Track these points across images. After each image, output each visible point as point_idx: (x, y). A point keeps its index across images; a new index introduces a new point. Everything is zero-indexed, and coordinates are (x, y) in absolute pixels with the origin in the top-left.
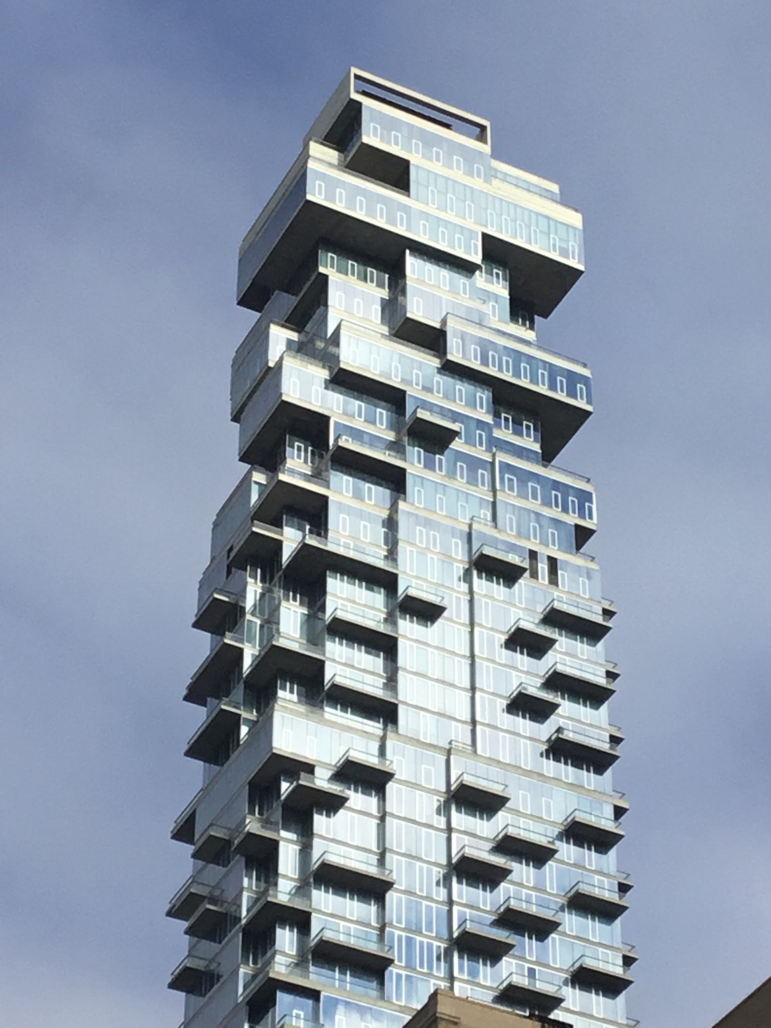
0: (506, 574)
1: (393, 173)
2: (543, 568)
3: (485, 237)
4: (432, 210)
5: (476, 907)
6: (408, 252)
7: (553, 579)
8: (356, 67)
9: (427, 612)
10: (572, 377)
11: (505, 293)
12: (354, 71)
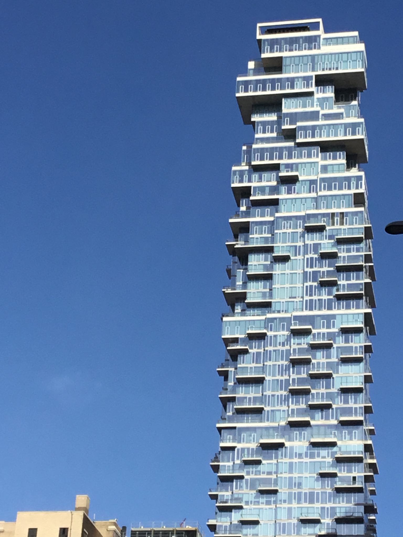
0: (321, 229)
1: (276, 65)
2: (337, 220)
6: (283, 99)
9: (285, 259)
11: (333, 95)
12: (259, 25)
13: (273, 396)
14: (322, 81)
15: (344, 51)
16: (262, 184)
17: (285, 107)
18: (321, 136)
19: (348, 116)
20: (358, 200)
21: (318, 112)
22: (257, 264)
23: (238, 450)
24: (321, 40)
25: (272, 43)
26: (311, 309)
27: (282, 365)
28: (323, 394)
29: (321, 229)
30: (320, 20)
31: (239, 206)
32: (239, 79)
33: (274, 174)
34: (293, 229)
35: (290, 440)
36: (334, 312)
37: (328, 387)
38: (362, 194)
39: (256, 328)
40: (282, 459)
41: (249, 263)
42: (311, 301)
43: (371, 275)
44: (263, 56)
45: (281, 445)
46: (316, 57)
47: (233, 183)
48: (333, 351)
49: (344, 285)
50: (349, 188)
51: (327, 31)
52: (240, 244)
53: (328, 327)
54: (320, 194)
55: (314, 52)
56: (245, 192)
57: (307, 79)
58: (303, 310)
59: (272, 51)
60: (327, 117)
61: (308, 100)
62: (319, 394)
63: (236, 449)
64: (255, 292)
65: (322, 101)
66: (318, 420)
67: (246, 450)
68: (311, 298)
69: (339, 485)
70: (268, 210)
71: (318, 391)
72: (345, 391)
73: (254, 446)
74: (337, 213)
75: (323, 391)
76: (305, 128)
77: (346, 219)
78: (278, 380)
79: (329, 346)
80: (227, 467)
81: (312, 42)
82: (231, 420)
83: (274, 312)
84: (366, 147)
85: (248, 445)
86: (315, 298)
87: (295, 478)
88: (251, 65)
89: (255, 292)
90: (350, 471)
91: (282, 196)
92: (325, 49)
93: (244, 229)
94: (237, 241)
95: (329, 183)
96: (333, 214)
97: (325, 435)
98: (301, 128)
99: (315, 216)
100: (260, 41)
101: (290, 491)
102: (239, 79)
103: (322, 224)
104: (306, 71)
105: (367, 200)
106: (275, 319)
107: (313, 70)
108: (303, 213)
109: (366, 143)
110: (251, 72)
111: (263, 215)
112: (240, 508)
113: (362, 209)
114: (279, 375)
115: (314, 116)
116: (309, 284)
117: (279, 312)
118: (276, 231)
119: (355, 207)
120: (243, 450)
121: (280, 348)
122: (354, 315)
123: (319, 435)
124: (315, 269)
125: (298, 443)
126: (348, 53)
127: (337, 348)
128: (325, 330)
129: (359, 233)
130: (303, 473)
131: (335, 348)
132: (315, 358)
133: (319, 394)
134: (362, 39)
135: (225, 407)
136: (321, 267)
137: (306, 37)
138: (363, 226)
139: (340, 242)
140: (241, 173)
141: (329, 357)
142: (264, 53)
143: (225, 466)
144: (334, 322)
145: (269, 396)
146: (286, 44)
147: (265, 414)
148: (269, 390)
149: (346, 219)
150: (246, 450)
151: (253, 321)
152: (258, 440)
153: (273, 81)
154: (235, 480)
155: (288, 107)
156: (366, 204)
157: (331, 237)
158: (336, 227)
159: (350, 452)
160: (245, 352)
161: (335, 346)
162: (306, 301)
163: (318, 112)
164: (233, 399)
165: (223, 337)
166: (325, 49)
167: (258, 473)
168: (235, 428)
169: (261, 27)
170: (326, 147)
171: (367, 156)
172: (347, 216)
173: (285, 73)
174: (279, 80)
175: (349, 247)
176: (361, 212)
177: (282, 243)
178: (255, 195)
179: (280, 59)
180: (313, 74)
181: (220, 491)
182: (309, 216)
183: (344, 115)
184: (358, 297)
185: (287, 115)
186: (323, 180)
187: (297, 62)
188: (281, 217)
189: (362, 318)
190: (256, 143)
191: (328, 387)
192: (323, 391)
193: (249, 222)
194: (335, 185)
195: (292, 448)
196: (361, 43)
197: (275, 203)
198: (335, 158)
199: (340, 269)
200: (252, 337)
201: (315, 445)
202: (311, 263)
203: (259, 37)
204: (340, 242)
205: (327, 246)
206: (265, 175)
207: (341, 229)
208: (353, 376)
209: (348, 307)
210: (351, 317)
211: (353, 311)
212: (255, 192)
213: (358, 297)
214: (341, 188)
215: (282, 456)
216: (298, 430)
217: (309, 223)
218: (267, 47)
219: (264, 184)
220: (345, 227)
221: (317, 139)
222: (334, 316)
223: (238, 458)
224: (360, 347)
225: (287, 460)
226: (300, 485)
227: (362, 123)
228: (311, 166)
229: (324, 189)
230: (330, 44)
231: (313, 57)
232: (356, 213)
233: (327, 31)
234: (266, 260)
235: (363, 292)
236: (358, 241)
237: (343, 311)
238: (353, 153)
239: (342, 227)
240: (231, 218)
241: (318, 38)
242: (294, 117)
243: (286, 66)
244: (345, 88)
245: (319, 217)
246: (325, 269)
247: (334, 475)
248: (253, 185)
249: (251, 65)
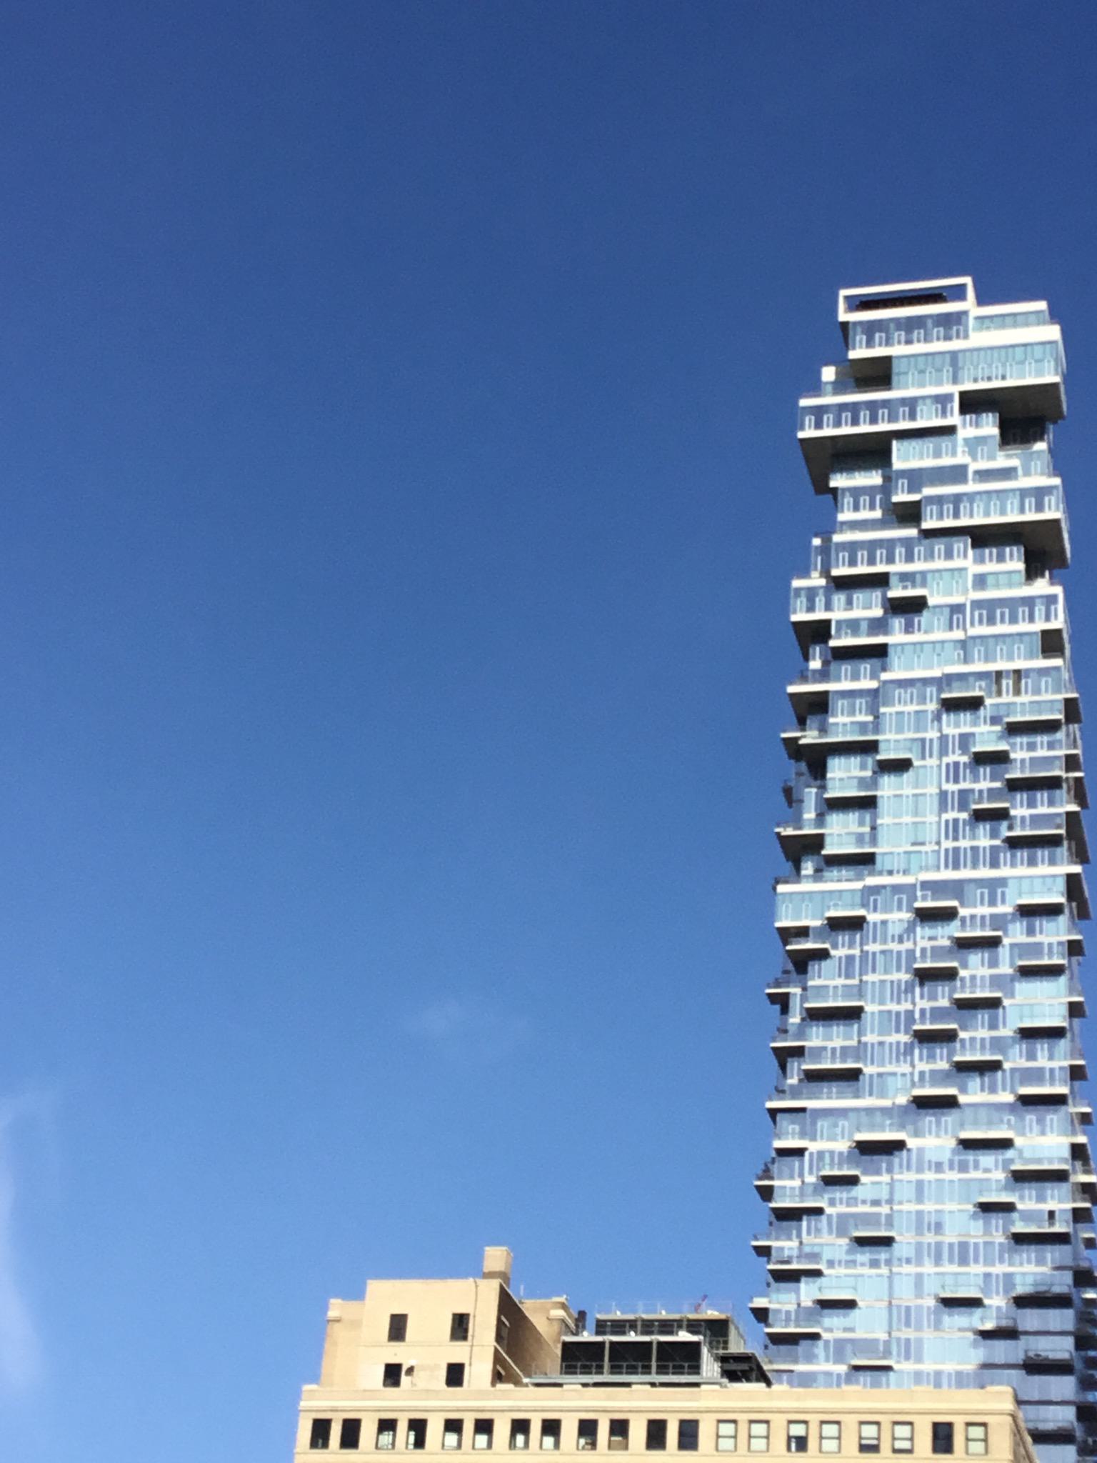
0: (974, 704)
1: (878, 374)
3: (962, 394)
5: (927, 1005)
7: (1017, 692)
9: (901, 766)
11: (995, 431)
12: (844, 293)
13: (881, 1044)
14: (972, 403)
15: (1018, 341)
17: (898, 457)
18: (971, 516)
19: (1027, 473)
20: (1050, 643)
21: (964, 468)
22: (844, 776)
23: (811, 1154)
24: (971, 322)
25: (871, 329)
26: (956, 866)
27: (899, 981)
28: (983, 1040)
29: (974, 704)
30: (967, 280)
31: (806, 658)
32: (804, 402)
33: (876, 595)
34: (918, 704)
35: (917, 1134)
36: (1004, 872)
37: (993, 1026)
38: (1059, 632)
39: (845, 907)
40: (901, 1173)
41: (829, 775)
42: (956, 850)
43: (1079, 792)
44: (853, 354)
45: (900, 1145)
46: (960, 356)
47: (795, 612)
48: (1004, 952)
49: (1023, 818)
50: (1032, 619)
51: (982, 300)
52: (810, 737)
53: (992, 903)
54: (972, 632)
56: (819, 631)
57: (943, 400)
58: (938, 868)
59: (870, 344)
60: (984, 475)
61: (944, 442)
62: (975, 1039)
63: (807, 1154)
64: (841, 834)
65: (974, 445)
66: (973, 1093)
67: (827, 1155)
68: (956, 844)
69: (1020, 1227)
70: (866, 666)
71: (972, 1034)
72: (1029, 1034)
73: (843, 1146)
74: (1008, 672)
75: (983, 1033)
76: (939, 500)
77: (1026, 683)
78: (889, 1012)
79: (993, 943)
80: (790, 1189)
81: (951, 323)
82: (795, 1094)
83: (880, 873)
84: (1066, 536)
85: (831, 1145)
86: (964, 843)
87: (929, 1212)
88: (828, 374)
89: (841, 834)
90: (1041, 1198)
91: (895, 637)
92: (978, 339)
93: (817, 706)
94: (804, 730)
95: (990, 610)
96: (999, 675)
97: (990, 1124)
98: (931, 500)
99: (962, 677)
100: (845, 325)
101: (920, 1239)
102: (804, 402)
103: (977, 693)
104: (939, 383)
105: (1070, 642)
106: (884, 887)
107: (955, 380)
108: (937, 673)
109: (1065, 527)
110: (829, 388)
111: (855, 677)
112: (817, 1273)
113: (1058, 662)
114: (892, 999)
115: (958, 473)
116: (951, 815)
117: (890, 873)
118: (882, 710)
119: (1045, 657)
120: (821, 1154)
121: (894, 946)
122: (1044, 878)
123: (976, 1124)
125: (933, 1140)
126: (1025, 345)
127: (1012, 946)
128: (986, 910)
129: (1052, 712)
130: (943, 1203)
131: (1007, 948)
132: (965, 966)
133: (975, 1039)
134: (1055, 315)
135: (783, 1067)
136: (976, 779)
137: (939, 315)
138: (1061, 697)
139: (1015, 729)
140: (811, 593)
141: (994, 963)
142: (854, 348)
143: (785, 1187)
144: (1003, 894)
145: (873, 1045)
146: (898, 329)
147: (864, 1080)
148: (872, 1032)
149: (1026, 683)
150: (827, 1155)
151: (836, 892)
152: (851, 1135)
153: (873, 406)
154: (805, 1218)
155: (904, 457)
156: (1067, 652)
157: (995, 720)
158: (1005, 699)
159: (1039, 1161)
160: (823, 955)
161: (1006, 941)
162: (947, 850)
163: (964, 468)
164: (799, 1052)
165: (778, 924)
166: (978, 339)
167: (852, 1202)
168: (803, 1110)
169: (847, 298)
170: (983, 537)
171: (1069, 554)
172: (1027, 677)
173: (899, 388)
174: (885, 403)
175: (1032, 739)
176: (1057, 669)
177: (897, 733)
178: (839, 637)
179: (887, 361)
180: (955, 390)
181: (777, 1239)
182: (948, 680)
183: (1020, 472)
184: (1053, 841)
186: (977, 604)
187: (921, 366)
188: (892, 682)
189: (1061, 885)
190: (841, 531)
191: (993, 1026)
192: (983, 1033)
193: (826, 693)
194: (1002, 615)
195: (921, 1151)
196: (1053, 323)
197: (879, 652)
198: (1001, 558)
199: (1015, 786)
200: (838, 925)
201: (968, 1145)
202: (954, 772)
203: (843, 316)
204: (1015, 729)
205: (987, 738)
206: (859, 596)
207: (1015, 704)
208: (1045, 1003)
209: (1032, 862)
210: (1037, 882)
211: (1043, 869)
212: (838, 630)
213: (1053, 841)
214: (1014, 620)
215: (901, 1166)
216: (933, 1115)
217: (950, 692)
218: (861, 338)
219: (856, 613)
220: (1024, 698)
221: (964, 522)
222: (1003, 882)
223: (811, 1172)
224: (1060, 943)
225: (913, 1176)
226: (939, 1227)
227: (1056, 487)
228: (953, 576)
229: (981, 622)
230: (988, 328)
231: (954, 355)
233: (982, 300)
234: (863, 767)
235: (1062, 831)
236: (1051, 727)
238: (1039, 548)
239: (1018, 700)
240: (791, 683)
241: (964, 317)
242: (916, 478)
243: (899, 374)
244: (1021, 416)
245: (971, 679)
246: (985, 785)
247: (1008, 1208)
248: (836, 615)
249: (828, 374)
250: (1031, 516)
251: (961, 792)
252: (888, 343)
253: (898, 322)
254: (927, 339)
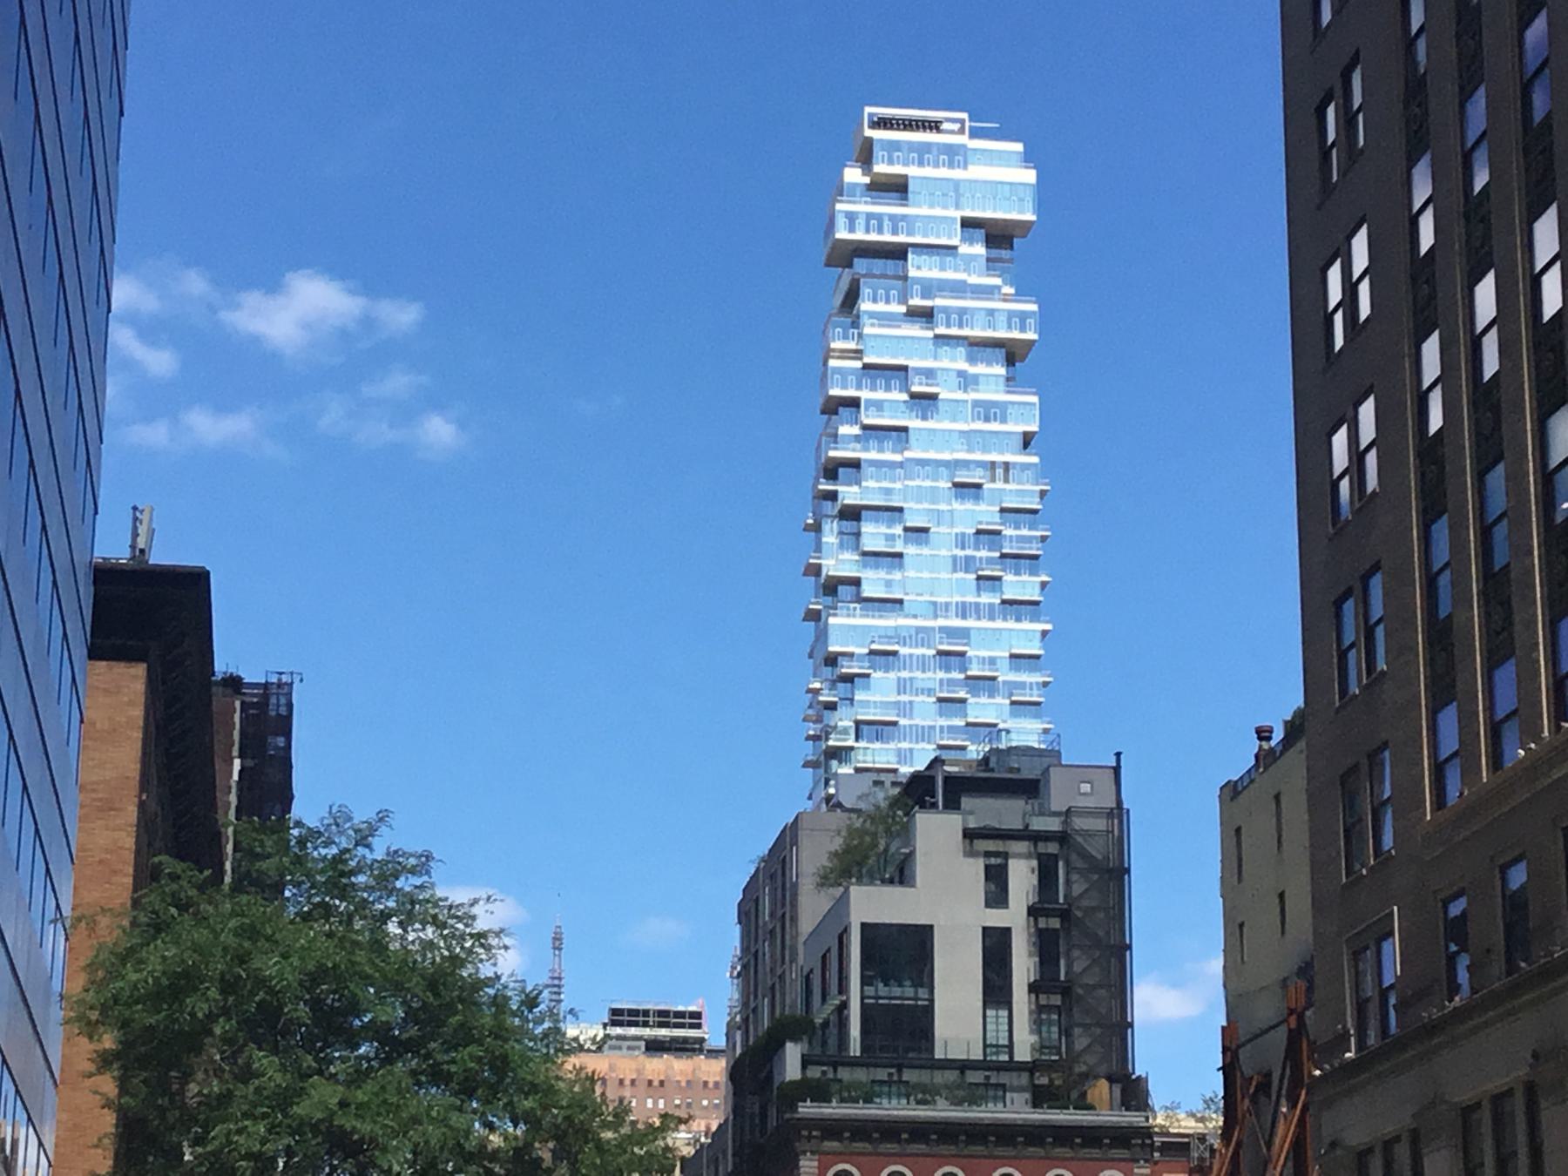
1: (897, 188)
4: (924, 211)
7: (1006, 481)
8: (870, 105)
10: (1023, 316)
12: (868, 110)
16: (885, 404)
22: (874, 534)
26: (964, 617)
36: (999, 624)
55: (957, 174)
83: (907, 616)
86: (971, 599)
91: (914, 423)
92: (976, 172)
96: (993, 463)
99: (965, 464)
107: (957, 207)
108: (946, 456)
115: (959, 289)
117: (915, 617)
124: (969, 552)
126: (1011, 184)
134: (1028, 159)
137: (945, 145)
138: (1038, 488)
153: (893, 218)
155: (920, 268)
166: (976, 172)
169: (870, 115)
170: (978, 347)
174: (904, 217)
180: (958, 214)
182: (958, 464)
185: (918, 280)
202: (961, 541)
203: (868, 133)
209: (1018, 620)
211: (1026, 625)
220: (1011, 486)
231: (957, 184)
232: (1025, 467)
237: (1011, 624)
239: (1008, 487)
242: (929, 288)
246: (984, 553)
250: (1016, 335)
251: (967, 557)
252: (906, 164)
253: (912, 146)
254: (936, 166)
